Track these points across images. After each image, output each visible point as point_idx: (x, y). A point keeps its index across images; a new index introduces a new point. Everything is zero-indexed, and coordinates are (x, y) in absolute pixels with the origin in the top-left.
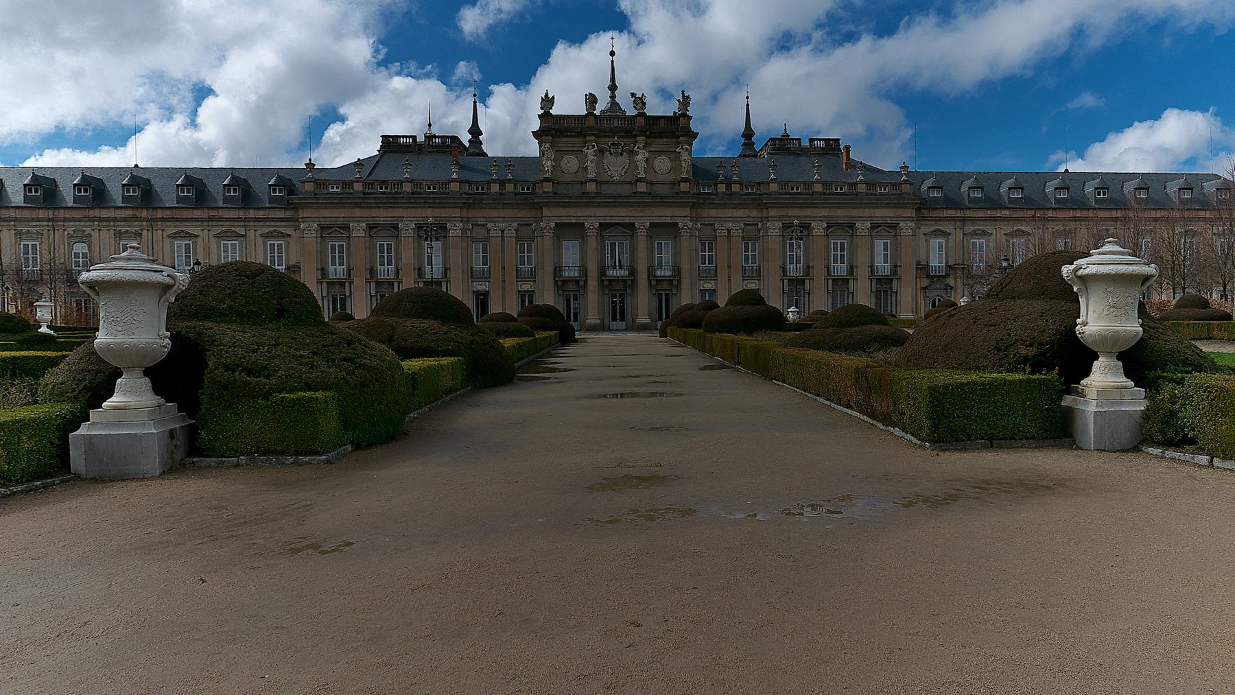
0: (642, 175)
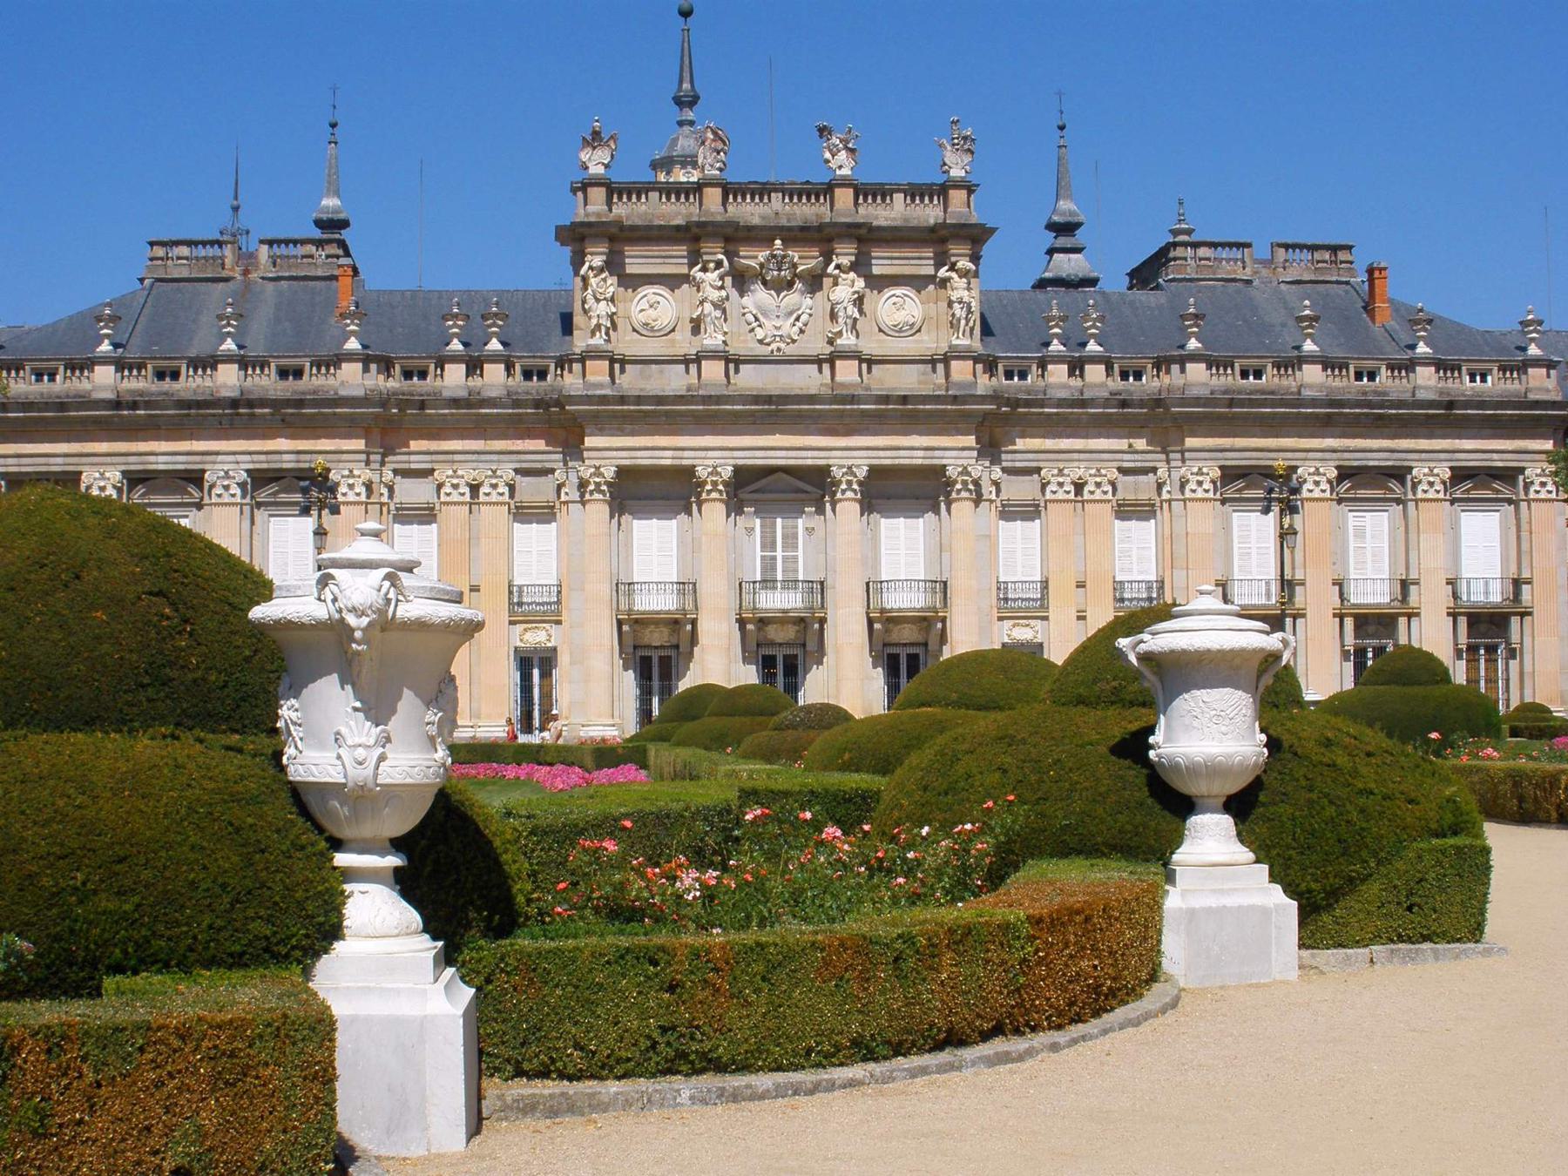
0: (847, 341)
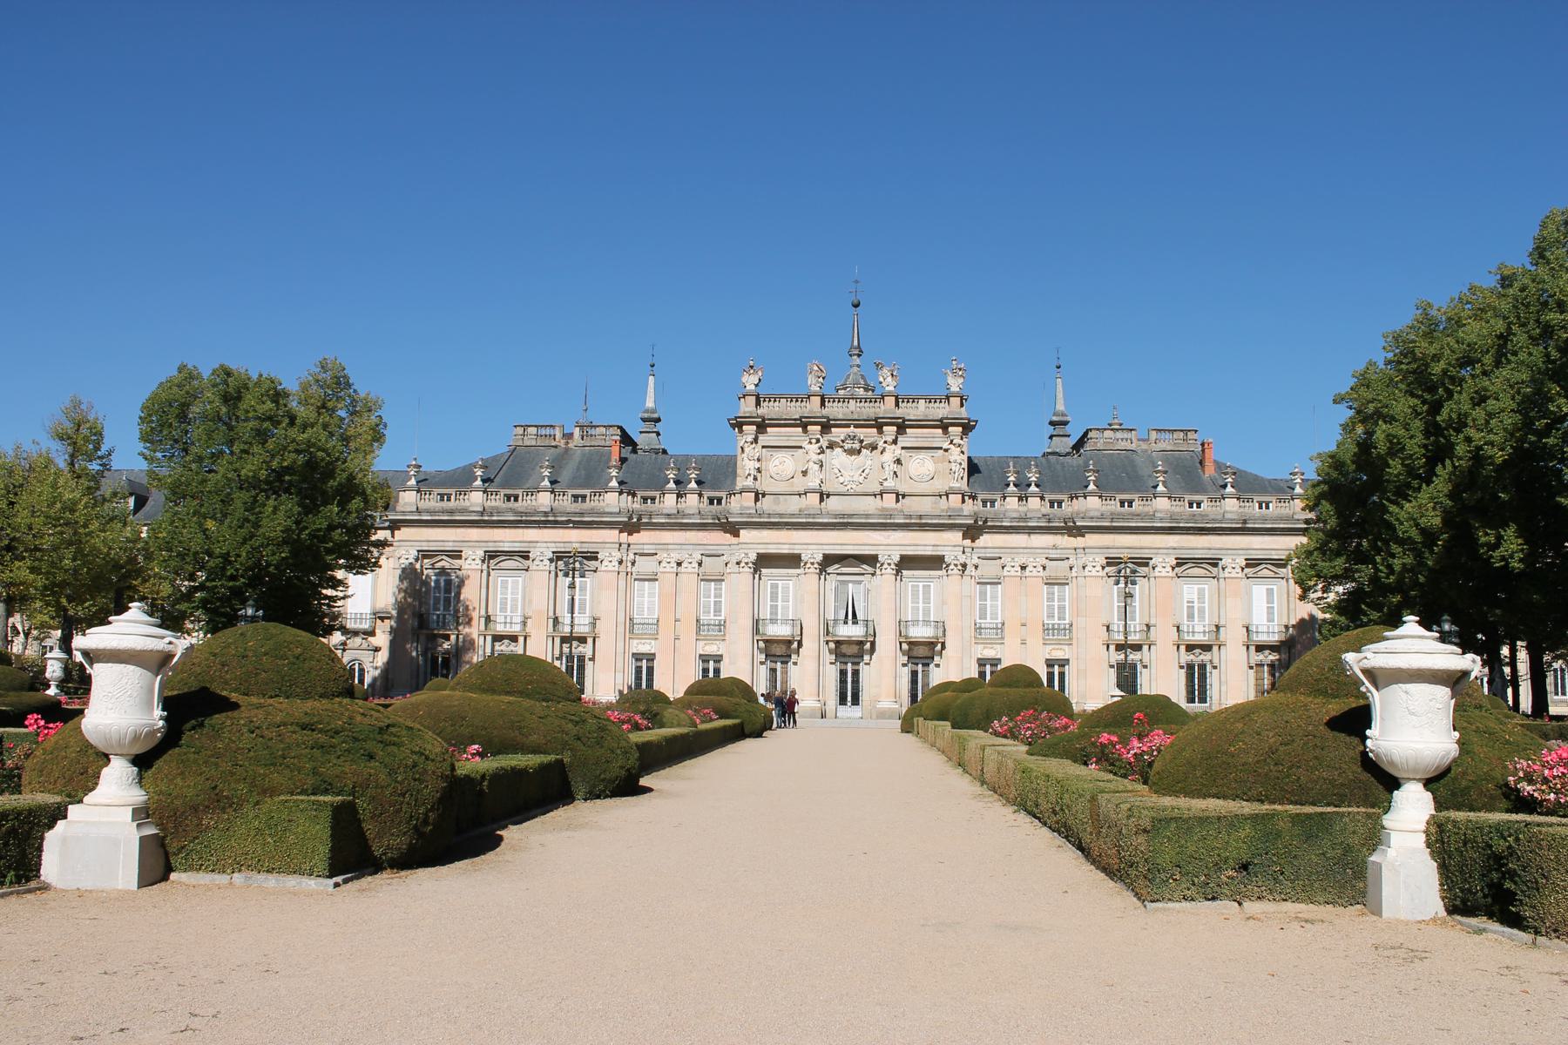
0: (890, 484)
